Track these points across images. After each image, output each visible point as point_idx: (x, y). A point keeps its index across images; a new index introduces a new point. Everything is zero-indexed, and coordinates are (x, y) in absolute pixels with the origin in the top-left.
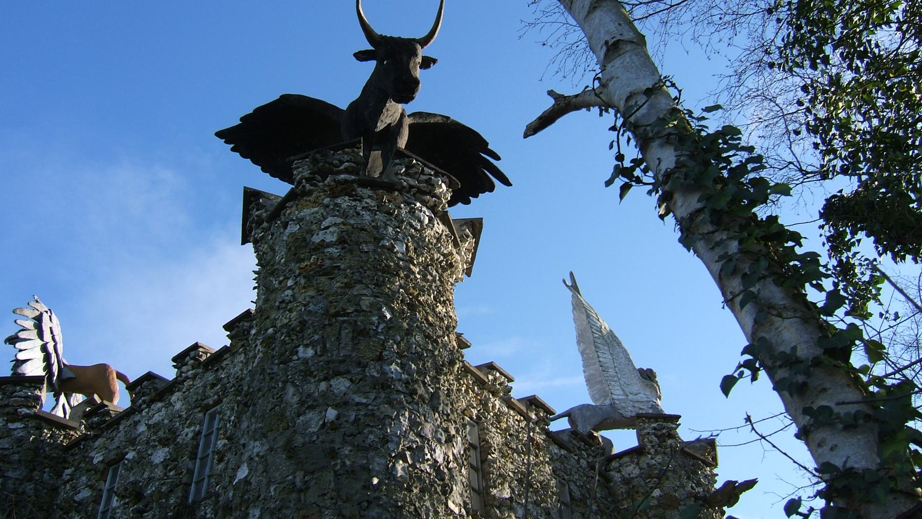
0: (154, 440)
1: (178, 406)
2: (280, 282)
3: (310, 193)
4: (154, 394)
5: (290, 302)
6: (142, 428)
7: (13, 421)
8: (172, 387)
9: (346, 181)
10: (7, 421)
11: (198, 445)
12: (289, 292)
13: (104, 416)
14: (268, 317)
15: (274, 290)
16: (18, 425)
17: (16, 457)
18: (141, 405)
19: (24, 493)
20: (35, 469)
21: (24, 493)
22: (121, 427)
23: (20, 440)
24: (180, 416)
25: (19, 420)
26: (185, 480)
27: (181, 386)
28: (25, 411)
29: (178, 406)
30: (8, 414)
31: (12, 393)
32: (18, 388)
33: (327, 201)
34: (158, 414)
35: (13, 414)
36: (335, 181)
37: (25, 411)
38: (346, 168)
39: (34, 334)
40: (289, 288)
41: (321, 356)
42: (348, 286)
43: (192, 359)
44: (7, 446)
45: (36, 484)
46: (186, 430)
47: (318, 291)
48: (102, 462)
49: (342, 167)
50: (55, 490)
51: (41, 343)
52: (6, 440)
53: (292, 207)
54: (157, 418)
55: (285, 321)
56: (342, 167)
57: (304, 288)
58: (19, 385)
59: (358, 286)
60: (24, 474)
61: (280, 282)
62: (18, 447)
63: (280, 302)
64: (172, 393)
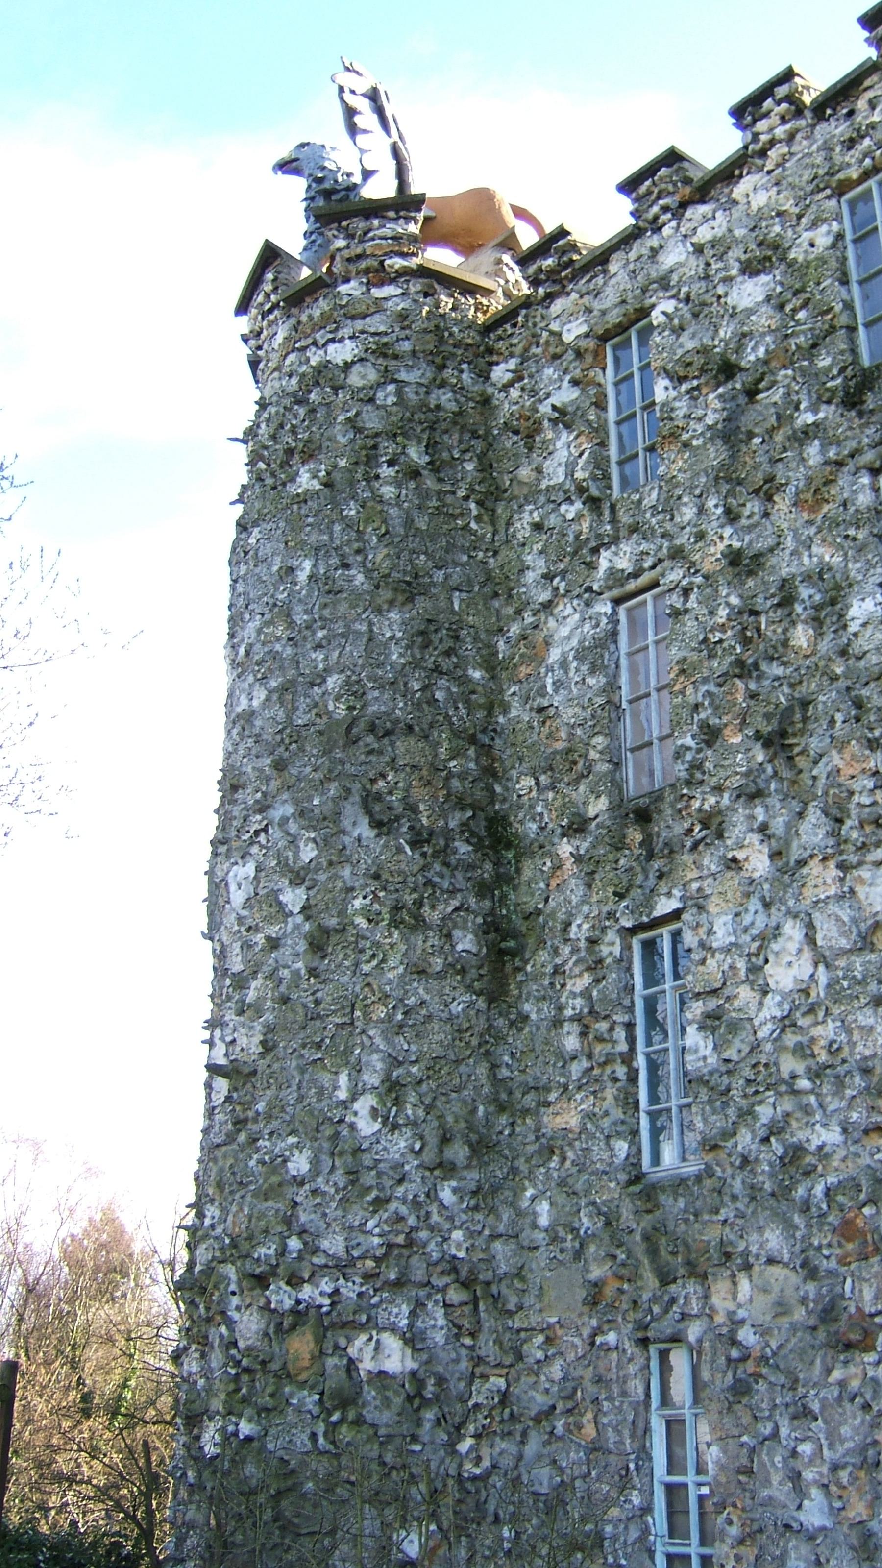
7: (381, 284)
13: (564, 253)
17: (406, 346)
19: (438, 407)
21: (438, 407)
23: (403, 316)
25: (392, 281)
28: (398, 263)
30: (367, 271)
31: (365, 233)
32: (376, 222)
35: (377, 271)
37: (398, 263)
44: (382, 329)
45: (454, 392)
51: (388, 142)
52: (377, 317)
58: (377, 217)
60: (429, 375)
62: (403, 328)
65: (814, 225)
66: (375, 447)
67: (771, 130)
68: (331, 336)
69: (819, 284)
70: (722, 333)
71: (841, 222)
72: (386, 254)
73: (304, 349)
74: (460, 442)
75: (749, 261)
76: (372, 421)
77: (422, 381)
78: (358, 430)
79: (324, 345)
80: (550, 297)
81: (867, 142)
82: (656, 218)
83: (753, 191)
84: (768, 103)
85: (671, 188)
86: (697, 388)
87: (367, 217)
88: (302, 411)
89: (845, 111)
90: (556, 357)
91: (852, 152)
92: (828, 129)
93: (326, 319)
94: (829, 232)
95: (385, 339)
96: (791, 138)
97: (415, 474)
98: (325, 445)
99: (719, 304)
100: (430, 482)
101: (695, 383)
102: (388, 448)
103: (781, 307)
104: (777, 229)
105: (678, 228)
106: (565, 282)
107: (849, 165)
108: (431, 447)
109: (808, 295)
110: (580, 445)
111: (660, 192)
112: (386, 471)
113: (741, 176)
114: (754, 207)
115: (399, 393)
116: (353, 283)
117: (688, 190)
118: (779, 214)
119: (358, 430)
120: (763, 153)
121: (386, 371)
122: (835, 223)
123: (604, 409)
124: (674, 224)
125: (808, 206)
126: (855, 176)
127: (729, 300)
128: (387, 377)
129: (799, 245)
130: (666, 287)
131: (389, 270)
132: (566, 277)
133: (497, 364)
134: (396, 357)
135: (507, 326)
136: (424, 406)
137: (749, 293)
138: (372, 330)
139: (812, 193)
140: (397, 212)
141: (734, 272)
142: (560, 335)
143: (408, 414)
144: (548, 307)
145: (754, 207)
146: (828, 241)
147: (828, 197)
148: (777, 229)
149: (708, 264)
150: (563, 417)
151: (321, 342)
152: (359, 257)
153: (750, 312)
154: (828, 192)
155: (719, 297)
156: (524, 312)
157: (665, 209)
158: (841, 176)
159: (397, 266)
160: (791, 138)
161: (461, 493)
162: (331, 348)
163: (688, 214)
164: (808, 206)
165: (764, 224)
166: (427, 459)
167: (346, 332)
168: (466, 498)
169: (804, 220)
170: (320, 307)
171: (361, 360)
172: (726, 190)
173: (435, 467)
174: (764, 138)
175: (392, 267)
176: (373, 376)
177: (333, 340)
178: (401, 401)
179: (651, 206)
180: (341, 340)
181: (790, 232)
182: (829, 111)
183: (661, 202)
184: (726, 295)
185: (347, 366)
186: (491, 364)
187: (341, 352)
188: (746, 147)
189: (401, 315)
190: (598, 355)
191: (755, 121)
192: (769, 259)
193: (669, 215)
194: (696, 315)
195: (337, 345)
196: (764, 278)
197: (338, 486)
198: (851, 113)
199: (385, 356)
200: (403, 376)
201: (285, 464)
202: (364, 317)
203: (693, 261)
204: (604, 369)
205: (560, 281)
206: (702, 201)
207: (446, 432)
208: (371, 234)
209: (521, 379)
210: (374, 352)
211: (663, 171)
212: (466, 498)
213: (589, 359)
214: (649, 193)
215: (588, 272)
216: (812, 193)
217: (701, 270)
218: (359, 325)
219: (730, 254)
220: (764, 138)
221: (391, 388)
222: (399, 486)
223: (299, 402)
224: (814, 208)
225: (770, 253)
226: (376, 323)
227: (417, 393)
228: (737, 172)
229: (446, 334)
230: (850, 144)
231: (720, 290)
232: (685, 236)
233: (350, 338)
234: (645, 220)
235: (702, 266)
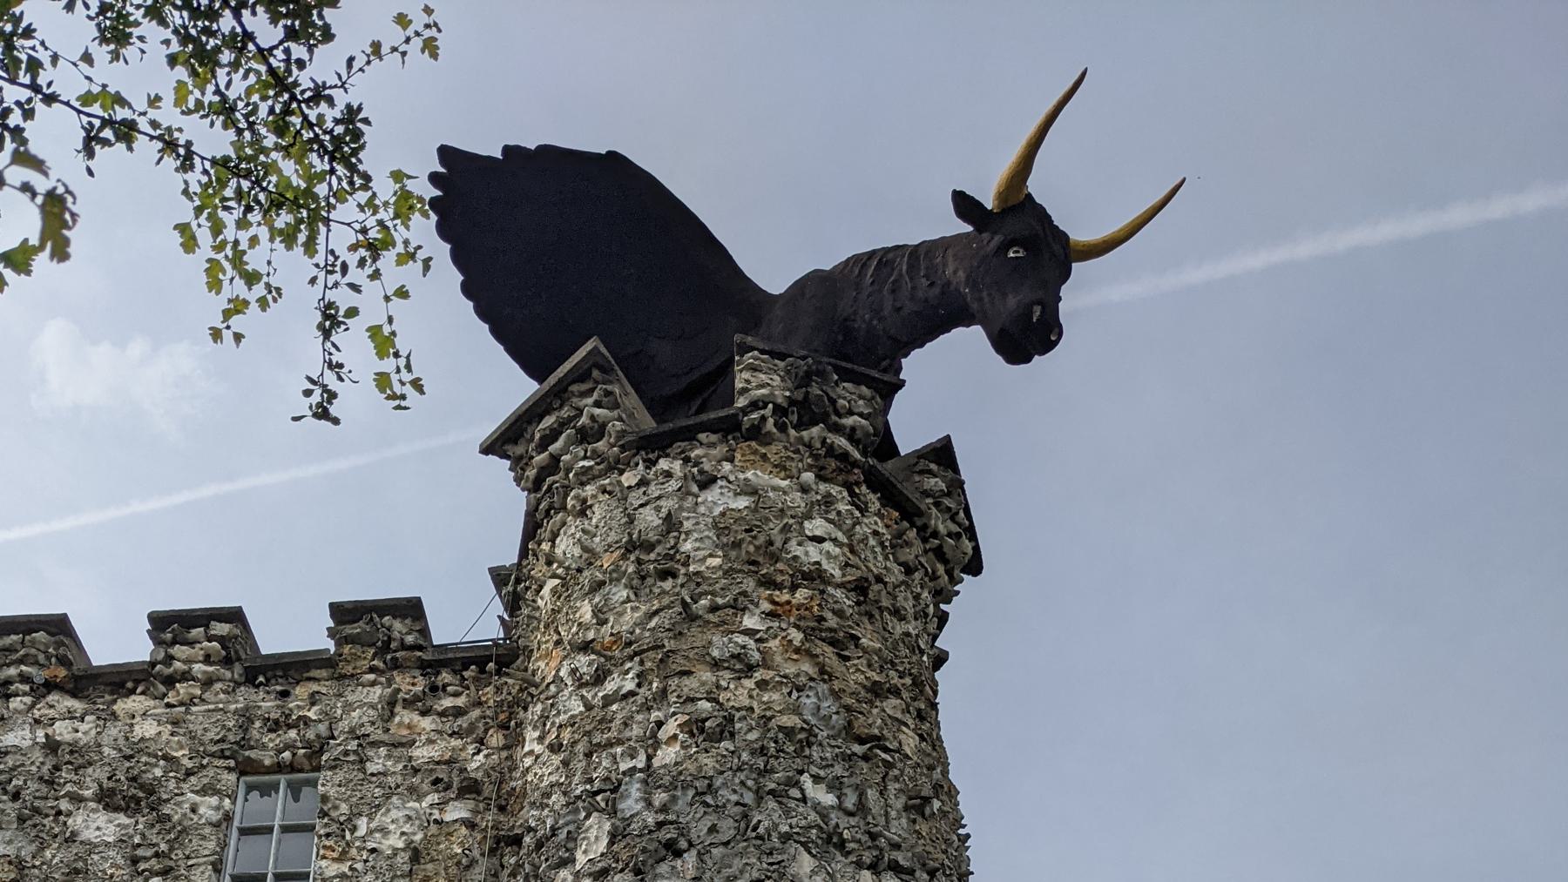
3: (767, 440)
9: (844, 457)
33: (808, 477)
36: (824, 441)
38: (853, 429)
41: (851, 814)
42: (877, 691)
47: (822, 671)
49: (849, 421)
53: (712, 445)
56: (849, 421)
57: (797, 651)
59: (894, 701)
65: (203, 791)
67: (188, 661)
69: (188, 858)
70: (48, 854)
71: (234, 803)
75: (112, 792)
81: (293, 734)
83: (143, 717)
84: (197, 632)
85: (41, 657)
89: (279, 688)
91: (273, 736)
92: (254, 697)
94: (218, 808)
96: (208, 683)
99: (56, 821)
103: (135, 861)
104: (158, 772)
107: (264, 747)
109: (172, 864)
111: (26, 655)
113: (133, 692)
114: (138, 732)
117: (62, 673)
118: (165, 757)
120: (170, 682)
122: (227, 801)
124: (28, 700)
125: (203, 767)
126: (267, 762)
127: (70, 822)
129: (178, 804)
137: (98, 826)
139: (212, 755)
141: (88, 793)
145: (138, 732)
146: (216, 817)
147: (229, 769)
148: (158, 772)
149: (57, 768)
153: (91, 847)
154: (232, 763)
155: (59, 813)
157: (24, 679)
158: (252, 754)
160: (208, 683)
163: (52, 698)
164: (203, 767)
165: (144, 759)
169: (193, 779)
172: (108, 698)
174: (178, 665)
179: (8, 665)
181: (172, 784)
182: (261, 679)
183: (23, 668)
184: (69, 814)
188: (153, 664)
191: (174, 642)
192: (138, 801)
193: (27, 688)
194: (21, 820)
196: (122, 819)
198: (284, 694)
203: (38, 756)
211: (40, 636)
214: (10, 649)
216: (212, 755)
217: (45, 769)
219: (90, 770)
220: (178, 665)
225: (141, 794)
228: (130, 685)
230: (275, 726)
231: (64, 805)
232: (37, 721)
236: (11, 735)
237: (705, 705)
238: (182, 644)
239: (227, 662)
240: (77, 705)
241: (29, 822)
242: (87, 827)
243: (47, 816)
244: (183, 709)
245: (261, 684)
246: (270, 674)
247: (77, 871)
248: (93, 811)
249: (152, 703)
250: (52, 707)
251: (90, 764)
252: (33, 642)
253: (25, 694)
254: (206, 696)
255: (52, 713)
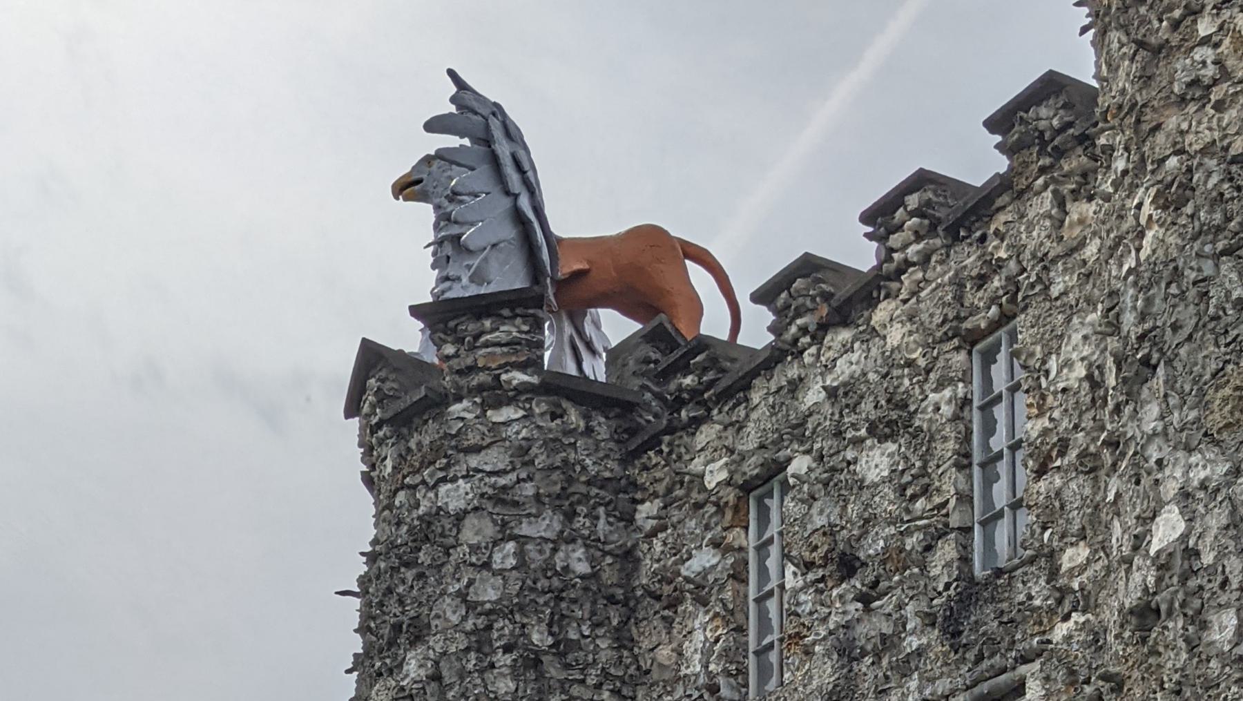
0: (854, 426)
1: (895, 335)
2: (1176, 25)
4: (824, 310)
5: (1215, 82)
6: (813, 395)
7: (497, 405)
8: (871, 289)
10: (485, 407)
11: (969, 432)
12: (1207, 53)
14: (1158, 127)
15: (1159, 51)
16: (509, 413)
17: (529, 489)
18: (796, 341)
20: (575, 514)
21: (566, 569)
22: (756, 397)
24: (910, 364)
25: (510, 401)
26: (955, 521)
27: (894, 285)
28: (518, 377)
29: (895, 335)
30: (481, 388)
31: (477, 337)
32: (488, 324)
34: (844, 355)
37: (518, 377)
39: (480, 179)
40: (1205, 41)
43: (912, 214)
46: (933, 397)
48: (728, 483)
50: (628, 557)
54: (844, 369)
55: (1207, 136)
58: (488, 316)
60: (557, 526)
61: (1176, 25)
63: (1190, 85)
64: (872, 303)
66: (489, 628)
68: (441, 474)
72: (500, 367)
73: (413, 487)
74: (593, 613)
76: (489, 593)
77: (548, 535)
78: (471, 607)
79: (435, 486)
80: (697, 422)
82: (796, 341)
86: (822, 579)
87: (479, 317)
88: (409, 575)
90: (698, 506)
93: (437, 450)
95: (502, 481)
96: (925, 260)
97: (533, 661)
98: (434, 623)
100: (554, 671)
101: (820, 573)
102: (504, 628)
105: (818, 356)
106: (710, 404)
108: (556, 623)
110: (718, 627)
112: (504, 660)
115: (520, 554)
116: (465, 403)
119: (471, 607)
121: (504, 524)
123: (745, 581)
124: (813, 350)
127: (858, 469)
128: (505, 533)
130: (802, 439)
131: (506, 386)
132: (710, 398)
133: (642, 501)
134: (516, 504)
135: (651, 453)
136: (548, 569)
137: (876, 462)
138: (488, 468)
140: (512, 310)
142: (702, 476)
143: (529, 582)
144: (694, 434)
150: (701, 592)
151: (431, 482)
152: (472, 369)
155: (849, 463)
156: (667, 438)
157: (804, 330)
159: (515, 382)
160: (925, 260)
161: (591, 681)
162: (443, 489)
166: (550, 641)
167: (461, 469)
168: (598, 686)
170: (426, 436)
171: (476, 509)
172: (866, 314)
173: (561, 648)
175: (509, 382)
176: (490, 530)
177: (444, 480)
178: (522, 563)
179: (790, 324)
180: (454, 480)
183: (799, 322)
185: (460, 517)
186: (635, 502)
187: (455, 496)
189: (521, 447)
190: (739, 509)
195: (449, 486)
196: (891, 447)
197: (447, 681)
199: (503, 502)
200: (525, 529)
201: (392, 643)
202: (477, 449)
204: (746, 528)
205: (702, 403)
206: (845, 323)
207: (574, 601)
208: (482, 339)
209: (664, 528)
210: (490, 498)
212: (598, 686)
213: (729, 515)
215: (732, 397)
218: (474, 461)
221: (511, 546)
222: (515, 678)
223: (407, 565)
224: (941, 363)
226: (494, 459)
227: (541, 552)
229: (578, 468)
233: (463, 477)
234: (784, 342)
235: (837, 412)
236: (810, 393)
237: (1173, 162)
238: (893, 233)
239: (932, 230)
240: (845, 335)
241: (831, 484)
242: (869, 469)
243: (842, 470)
244: (914, 300)
245: (964, 238)
246: (967, 224)
247: (867, 521)
248: (871, 448)
249: (893, 305)
250: (830, 348)
251: (862, 397)
252: (797, 291)
253: (810, 345)
254: (929, 275)
255: (831, 354)
